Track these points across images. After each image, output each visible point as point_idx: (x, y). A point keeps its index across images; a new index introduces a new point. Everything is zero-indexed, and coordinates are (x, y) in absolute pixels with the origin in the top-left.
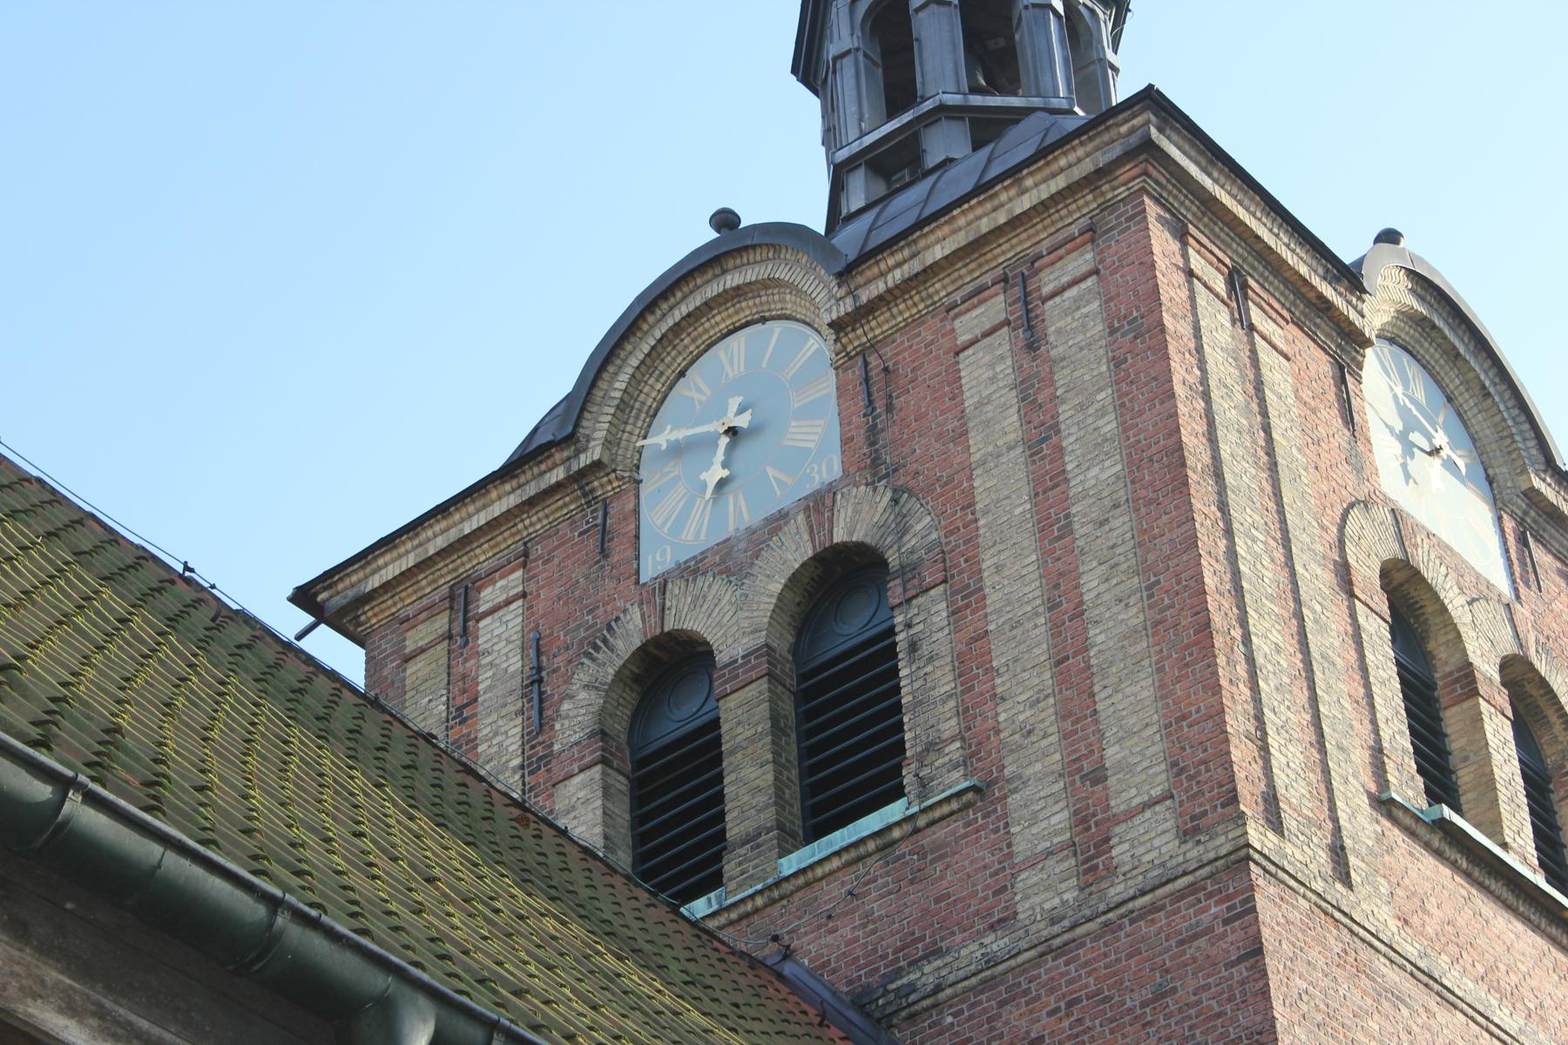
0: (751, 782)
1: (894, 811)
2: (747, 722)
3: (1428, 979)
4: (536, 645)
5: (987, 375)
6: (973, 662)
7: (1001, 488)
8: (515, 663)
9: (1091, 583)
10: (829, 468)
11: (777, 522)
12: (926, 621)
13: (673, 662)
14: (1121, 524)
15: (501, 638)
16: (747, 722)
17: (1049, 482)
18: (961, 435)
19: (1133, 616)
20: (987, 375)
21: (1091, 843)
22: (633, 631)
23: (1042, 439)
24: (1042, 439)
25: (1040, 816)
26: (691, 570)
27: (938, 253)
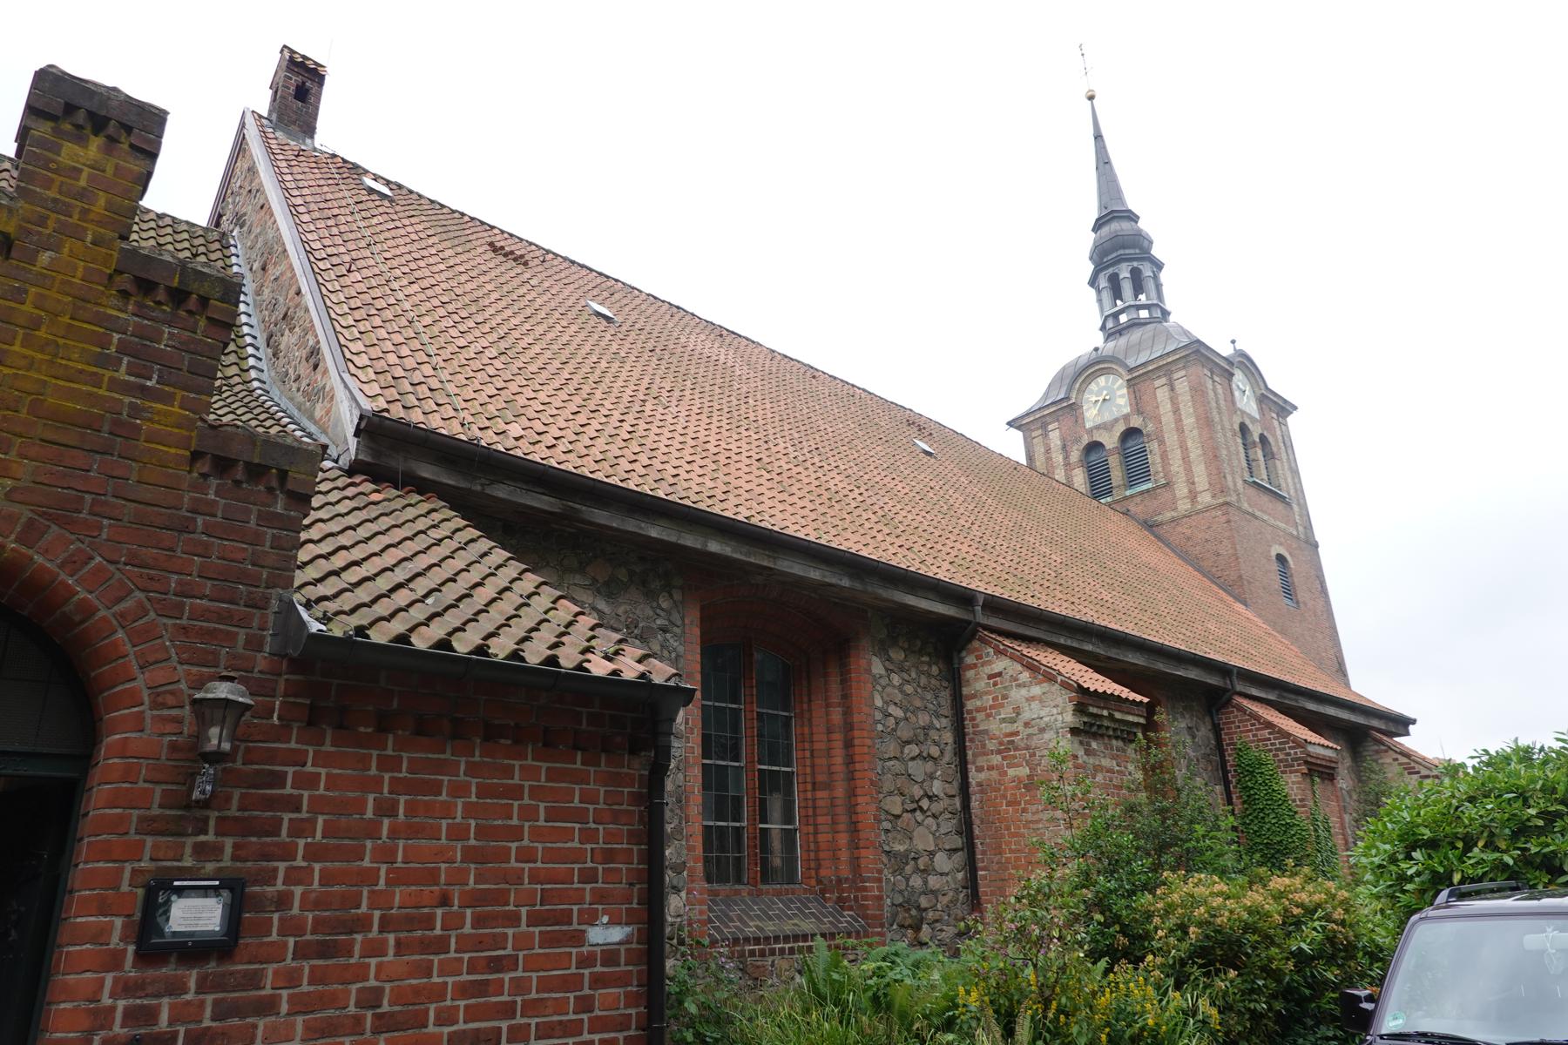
0: (1117, 475)
1: (1150, 485)
2: (1114, 462)
3: (1253, 515)
4: (1063, 440)
5: (1163, 395)
6: (1164, 456)
7: (1167, 418)
9: (1189, 444)
10: (1127, 410)
11: (1116, 420)
12: (1154, 446)
13: (1094, 446)
14: (1195, 432)
15: (1055, 437)
16: (1114, 462)
19: (1199, 452)
20: (1163, 395)
21: (1193, 495)
22: (1086, 440)
23: (1176, 411)
24: (1176, 411)
25: (1181, 490)
26: (1098, 427)
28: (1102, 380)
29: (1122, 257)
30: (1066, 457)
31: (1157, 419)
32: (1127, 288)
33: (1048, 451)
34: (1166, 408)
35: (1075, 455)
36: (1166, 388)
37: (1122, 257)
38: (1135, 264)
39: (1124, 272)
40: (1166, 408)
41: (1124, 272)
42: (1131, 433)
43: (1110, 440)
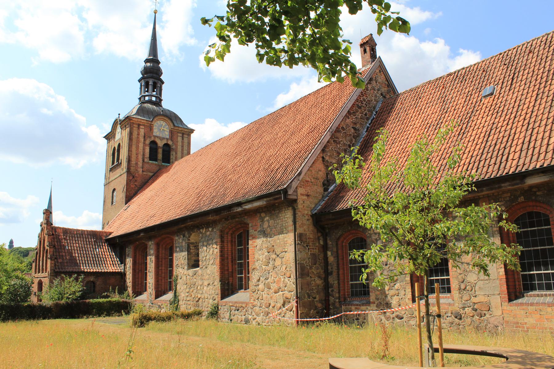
0: (160, 156)
2: (160, 151)
5: (180, 139)
7: (179, 148)
13: (153, 143)
16: (160, 151)
22: (152, 139)
23: (182, 146)
24: (182, 146)
29: (152, 76)
30: (145, 140)
32: (151, 88)
33: (138, 134)
34: (180, 144)
35: (148, 142)
36: (181, 138)
37: (152, 76)
38: (156, 81)
39: (151, 83)
40: (180, 144)
41: (151, 83)
42: (166, 145)
43: (160, 144)
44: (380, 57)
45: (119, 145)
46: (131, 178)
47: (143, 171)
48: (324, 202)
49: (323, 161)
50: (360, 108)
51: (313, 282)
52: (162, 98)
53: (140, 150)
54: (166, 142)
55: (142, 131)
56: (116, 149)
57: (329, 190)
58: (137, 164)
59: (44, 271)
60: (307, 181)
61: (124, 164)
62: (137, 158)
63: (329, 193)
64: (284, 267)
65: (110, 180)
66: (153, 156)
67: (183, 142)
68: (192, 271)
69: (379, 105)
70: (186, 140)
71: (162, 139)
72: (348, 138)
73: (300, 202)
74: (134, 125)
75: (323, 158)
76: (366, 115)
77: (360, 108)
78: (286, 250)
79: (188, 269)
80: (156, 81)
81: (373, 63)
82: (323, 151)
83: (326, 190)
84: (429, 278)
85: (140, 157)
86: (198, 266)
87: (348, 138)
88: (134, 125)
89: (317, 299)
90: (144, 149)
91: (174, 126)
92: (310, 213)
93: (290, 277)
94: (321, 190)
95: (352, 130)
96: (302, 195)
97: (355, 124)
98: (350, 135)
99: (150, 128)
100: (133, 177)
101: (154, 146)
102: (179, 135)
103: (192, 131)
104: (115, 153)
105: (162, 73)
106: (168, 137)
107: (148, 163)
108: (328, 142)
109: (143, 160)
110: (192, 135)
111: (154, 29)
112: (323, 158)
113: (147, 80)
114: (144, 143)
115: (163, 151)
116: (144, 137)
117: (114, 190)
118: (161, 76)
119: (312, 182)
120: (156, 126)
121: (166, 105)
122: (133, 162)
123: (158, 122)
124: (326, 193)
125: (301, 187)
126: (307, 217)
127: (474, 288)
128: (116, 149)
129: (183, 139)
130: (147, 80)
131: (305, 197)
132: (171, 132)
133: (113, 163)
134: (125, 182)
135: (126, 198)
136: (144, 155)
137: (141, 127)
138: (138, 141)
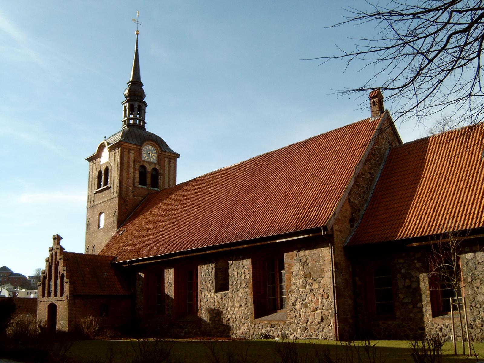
0: (149, 181)
2: (149, 175)
5: (167, 163)
7: (167, 172)
8: (133, 159)
12: (161, 178)
13: (143, 167)
16: (149, 175)
17: (169, 174)
18: (165, 167)
23: (169, 171)
24: (169, 171)
27: (167, 154)
28: (150, 147)
29: (136, 99)
30: (134, 165)
31: (164, 170)
33: (129, 159)
34: (167, 168)
35: (137, 167)
38: (141, 104)
40: (167, 168)
42: (154, 169)
43: (149, 168)
44: (387, 110)
45: (107, 169)
46: (122, 202)
47: (133, 196)
48: (351, 236)
49: (349, 202)
50: (374, 155)
51: (346, 302)
52: (146, 121)
53: (130, 175)
54: (154, 167)
55: (132, 156)
56: (103, 172)
57: (355, 227)
58: (127, 188)
59: (46, 295)
60: (340, 220)
61: (115, 188)
62: (128, 182)
63: (354, 229)
64: (321, 290)
65: (96, 203)
66: (142, 181)
67: (169, 167)
68: (219, 295)
69: (387, 152)
70: (172, 165)
71: (150, 163)
72: (366, 182)
73: (335, 236)
74: (125, 150)
75: (349, 200)
76: (378, 161)
77: (374, 155)
78: (323, 276)
79: (217, 291)
80: (141, 104)
81: (382, 116)
82: (349, 194)
83: (352, 226)
84: (459, 298)
85: (131, 181)
86: (228, 289)
87: (366, 182)
88: (125, 150)
89: (348, 317)
90: (134, 173)
91: (162, 151)
92: (342, 246)
93: (328, 298)
94: (348, 226)
95: (369, 176)
96: (336, 231)
97: (371, 169)
98: (367, 179)
99: (139, 153)
100: (125, 201)
101: (143, 170)
102: (166, 159)
103: (178, 156)
104: (102, 177)
105: (145, 96)
106: (156, 162)
107: (138, 187)
108: (352, 186)
109: (134, 185)
110: (178, 159)
111: (137, 50)
112: (349, 200)
113: (132, 103)
114: (134, 168)
115: (152, 175)
116: (134, 161)
117: (101, 213)
118: (144, 99)
119: (342, 220)
120: (144, 151)
121: (149, 128)
122: (124, 186)
123: (147, 147)
124: (352, 229)
125: (335, 225)
126: (340, 250)
127: (482, 305)
128: (103, 172)
129: (169, 164)
130: (132, 103)
131: (338, 233)
132: (159, 157)
133: (99, 186)
134: (117, 206)
135: (118, 221)
136: (134, 179)
137: (131, 151)
138: (129, 167)
